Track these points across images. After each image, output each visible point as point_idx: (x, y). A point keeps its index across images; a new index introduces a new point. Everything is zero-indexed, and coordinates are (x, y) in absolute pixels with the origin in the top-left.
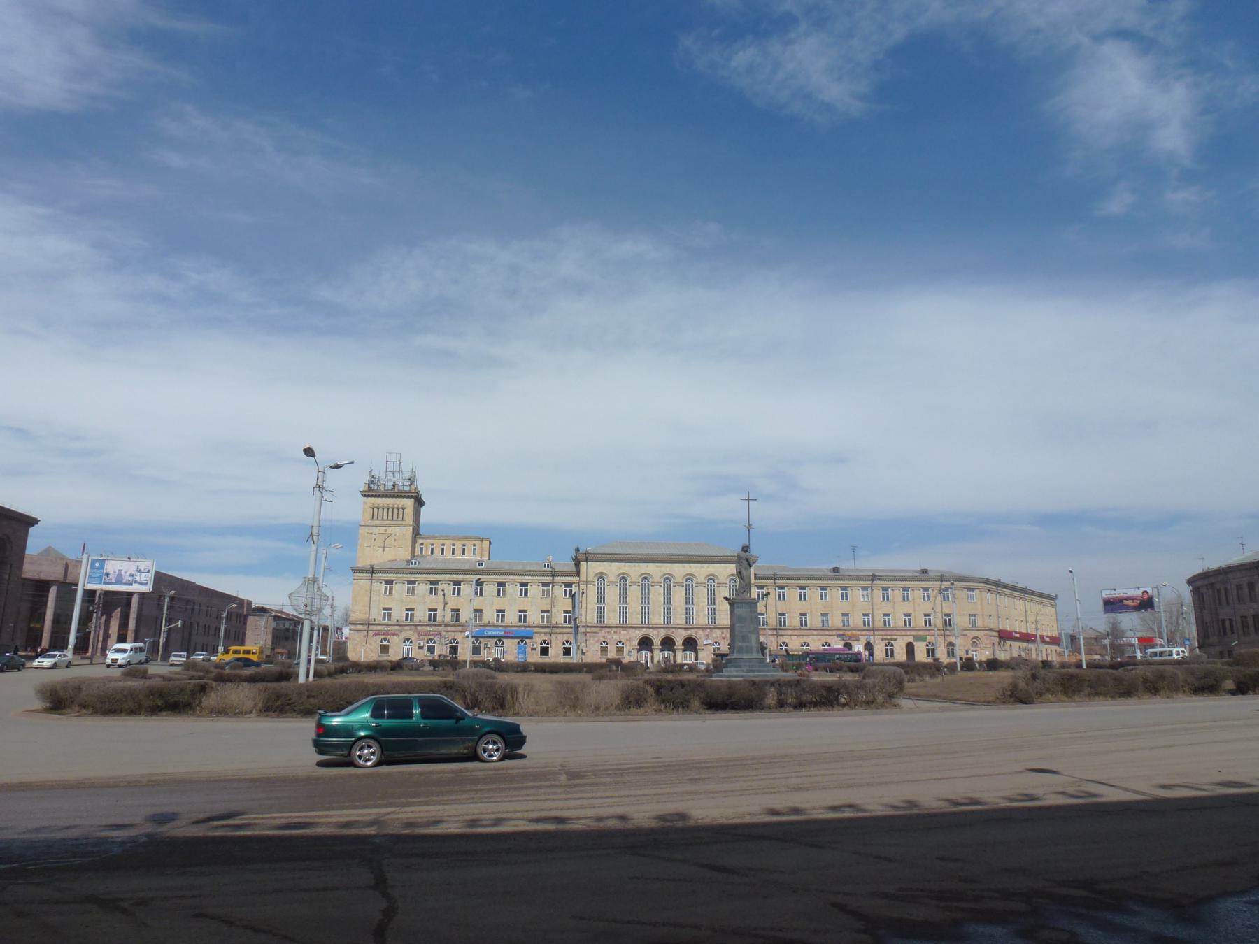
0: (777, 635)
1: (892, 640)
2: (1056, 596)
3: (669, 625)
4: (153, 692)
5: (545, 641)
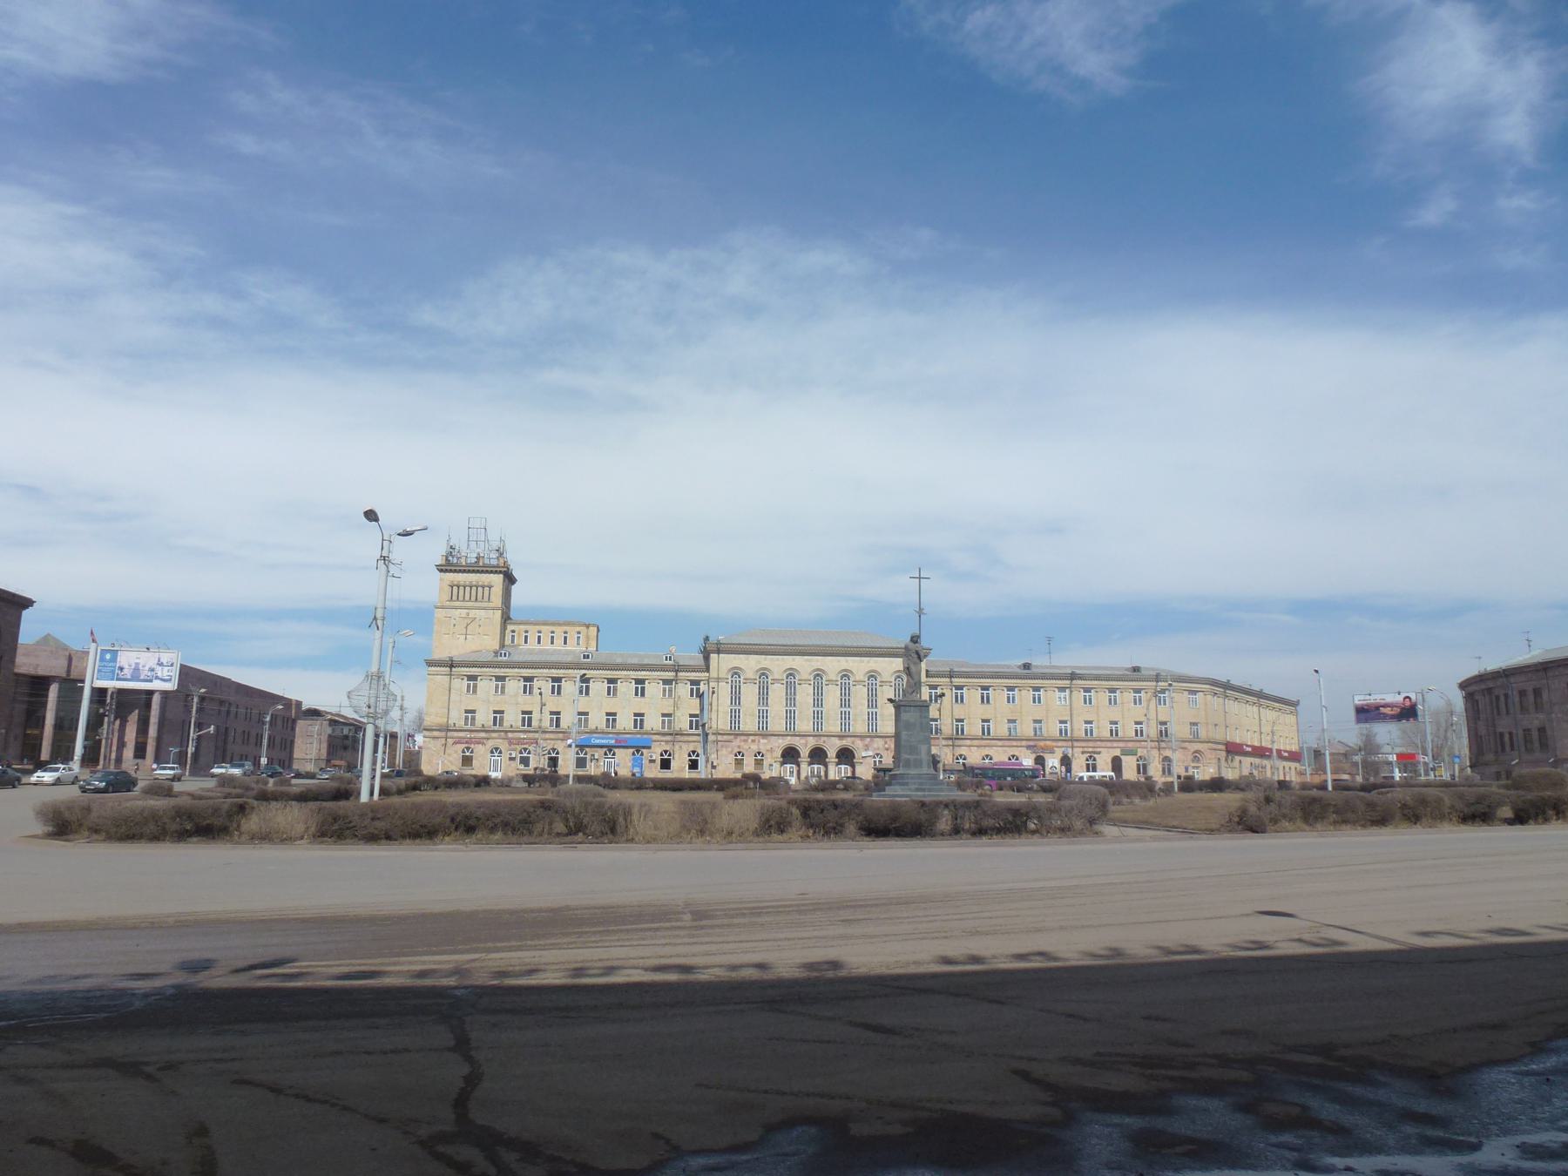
0: (953, 746)
1: (1095, 753)
2: (1298, 701)
3: (820, 732)
4: (179, 813)
5: (666, 752)
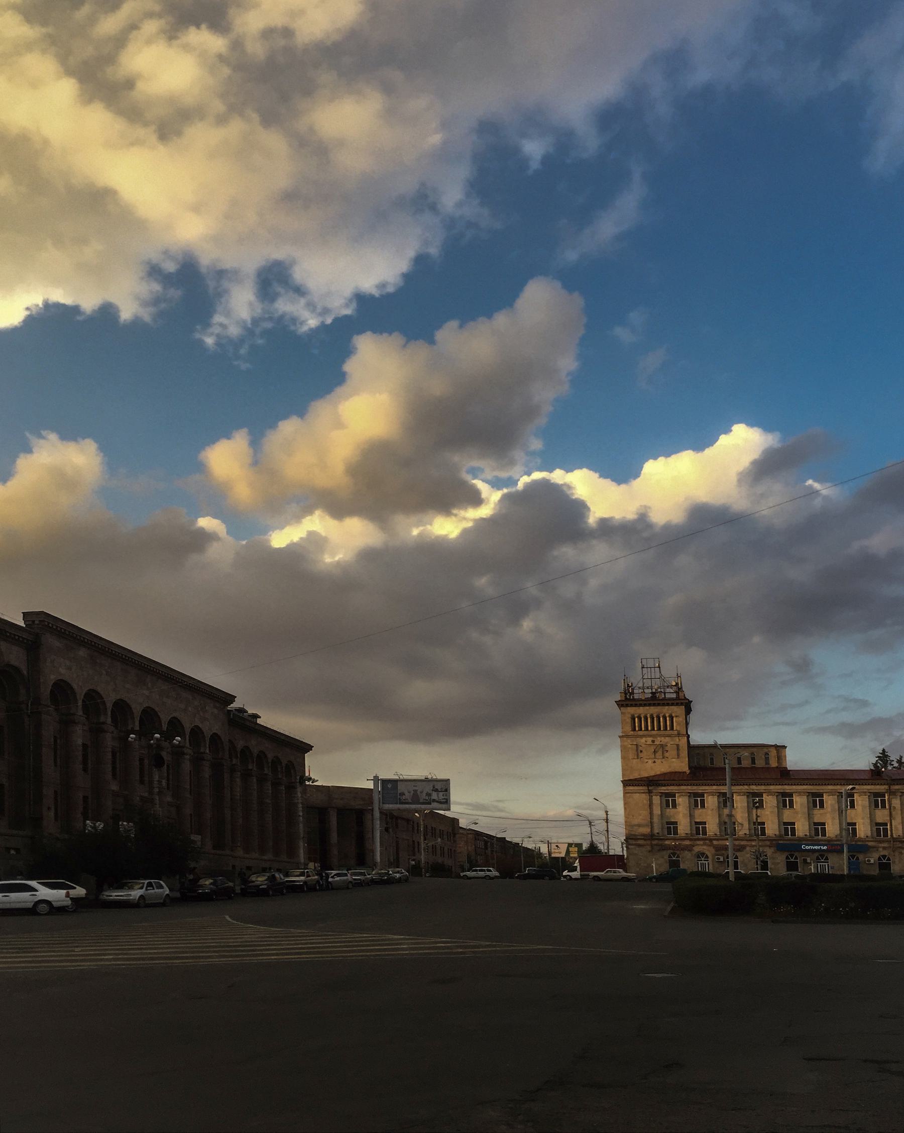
5: (884, 856)
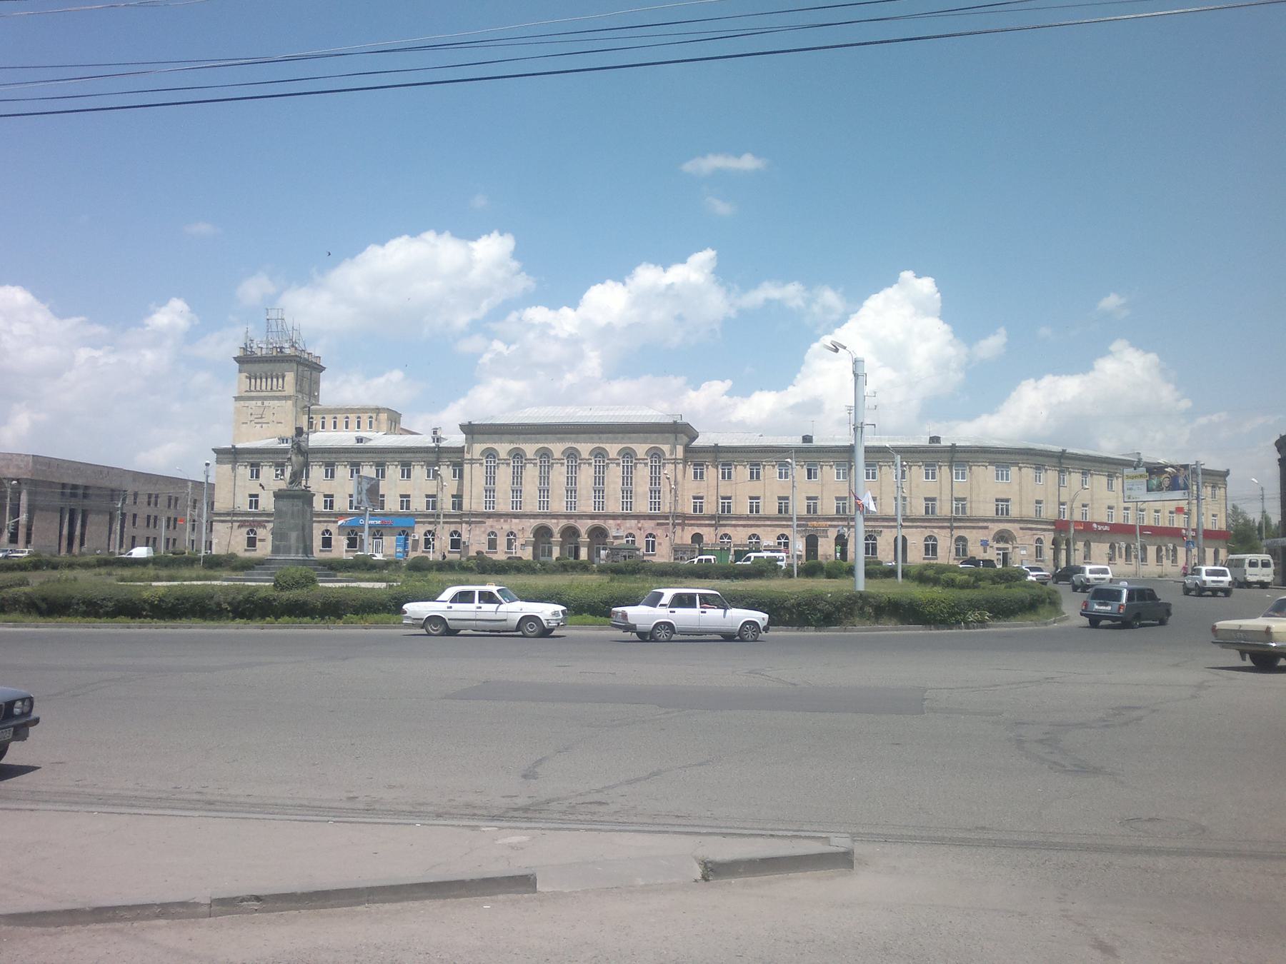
2: (1228, 471)
